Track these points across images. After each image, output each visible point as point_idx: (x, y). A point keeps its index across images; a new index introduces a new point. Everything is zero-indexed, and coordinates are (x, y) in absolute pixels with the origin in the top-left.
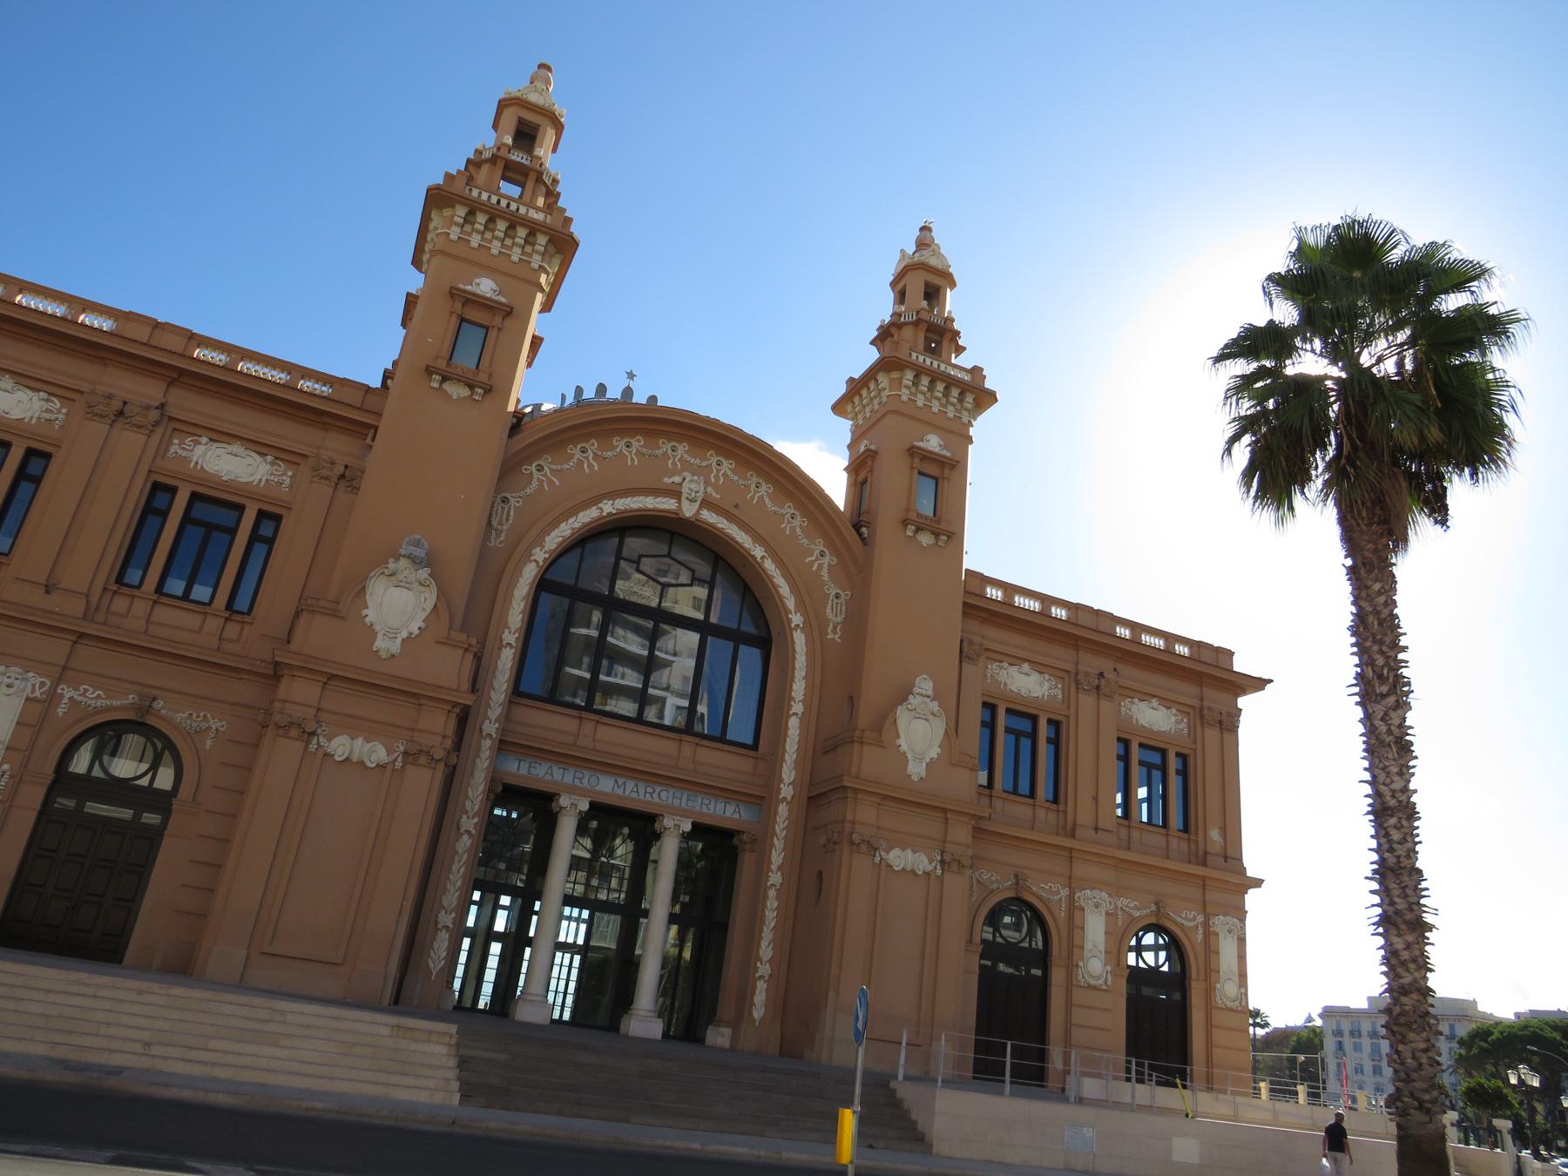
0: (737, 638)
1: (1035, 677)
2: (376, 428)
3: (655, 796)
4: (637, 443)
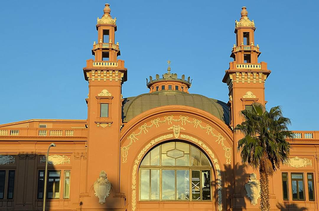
1: (301, 160)
4: (158, 120)
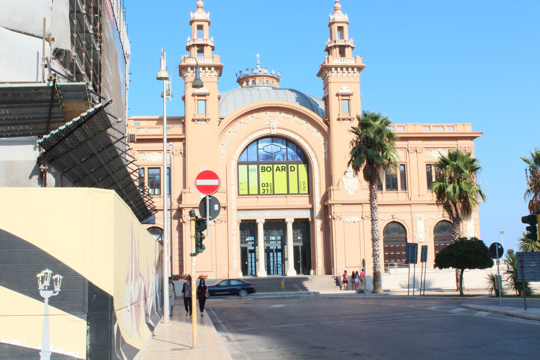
0: (298, 163)
2: (185, 138)
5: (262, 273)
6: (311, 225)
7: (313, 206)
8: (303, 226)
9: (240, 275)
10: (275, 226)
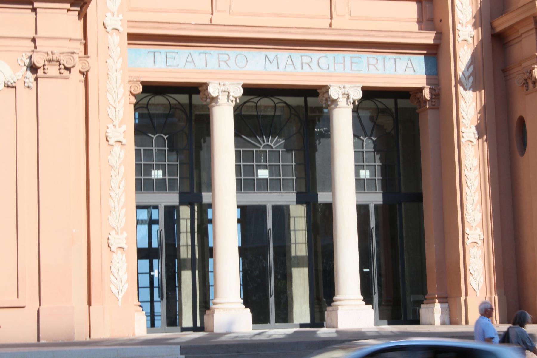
3: (314, 65)
5: (231, 316)
6: (428, 122)
7: (440, 35)
8: (398, 125)
9: (138, 327)
10: (285, 118)
